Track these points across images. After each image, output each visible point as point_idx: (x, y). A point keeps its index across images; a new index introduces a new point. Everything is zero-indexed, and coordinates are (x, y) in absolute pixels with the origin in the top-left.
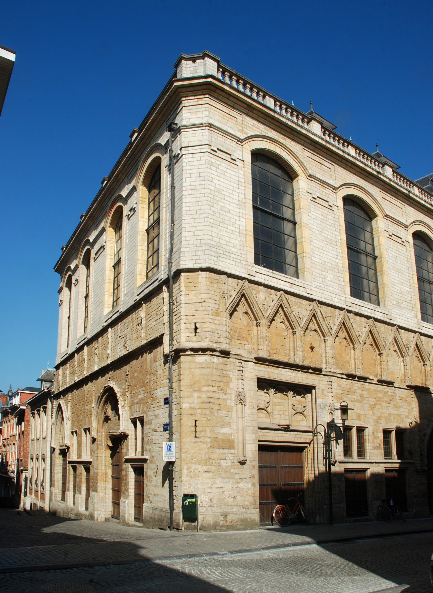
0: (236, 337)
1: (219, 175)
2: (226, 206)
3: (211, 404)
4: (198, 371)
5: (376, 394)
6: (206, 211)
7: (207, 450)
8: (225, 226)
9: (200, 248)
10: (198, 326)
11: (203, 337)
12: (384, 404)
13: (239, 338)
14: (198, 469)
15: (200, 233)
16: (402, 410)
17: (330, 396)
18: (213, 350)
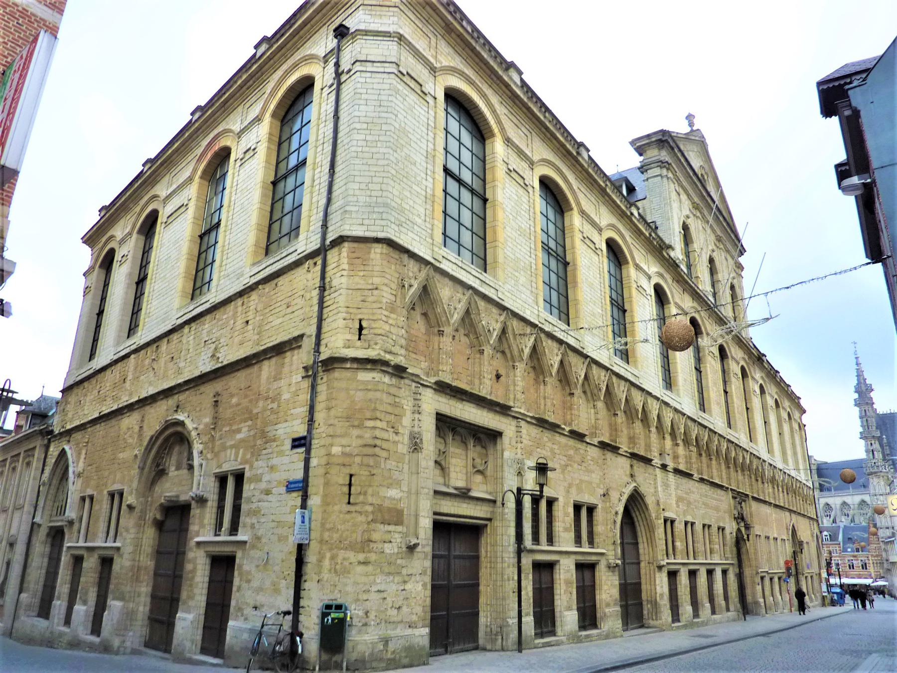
0: (411, 349)
1: (406, 109)
2: (412, 155)
3: (377, 449)
4: (360, 395)
5: (567, 450)
6: (387, 156)
7: (366, 526)
8: (409, 183)
9: (376, 210)
10: (364, 324)
11: (372, 343)
12: (576, 466)
13: (415, 351)
14: (348, 558)
15: (377, 187)
16: (593, 475)
17: (519, 447)
18: (386, 363)
